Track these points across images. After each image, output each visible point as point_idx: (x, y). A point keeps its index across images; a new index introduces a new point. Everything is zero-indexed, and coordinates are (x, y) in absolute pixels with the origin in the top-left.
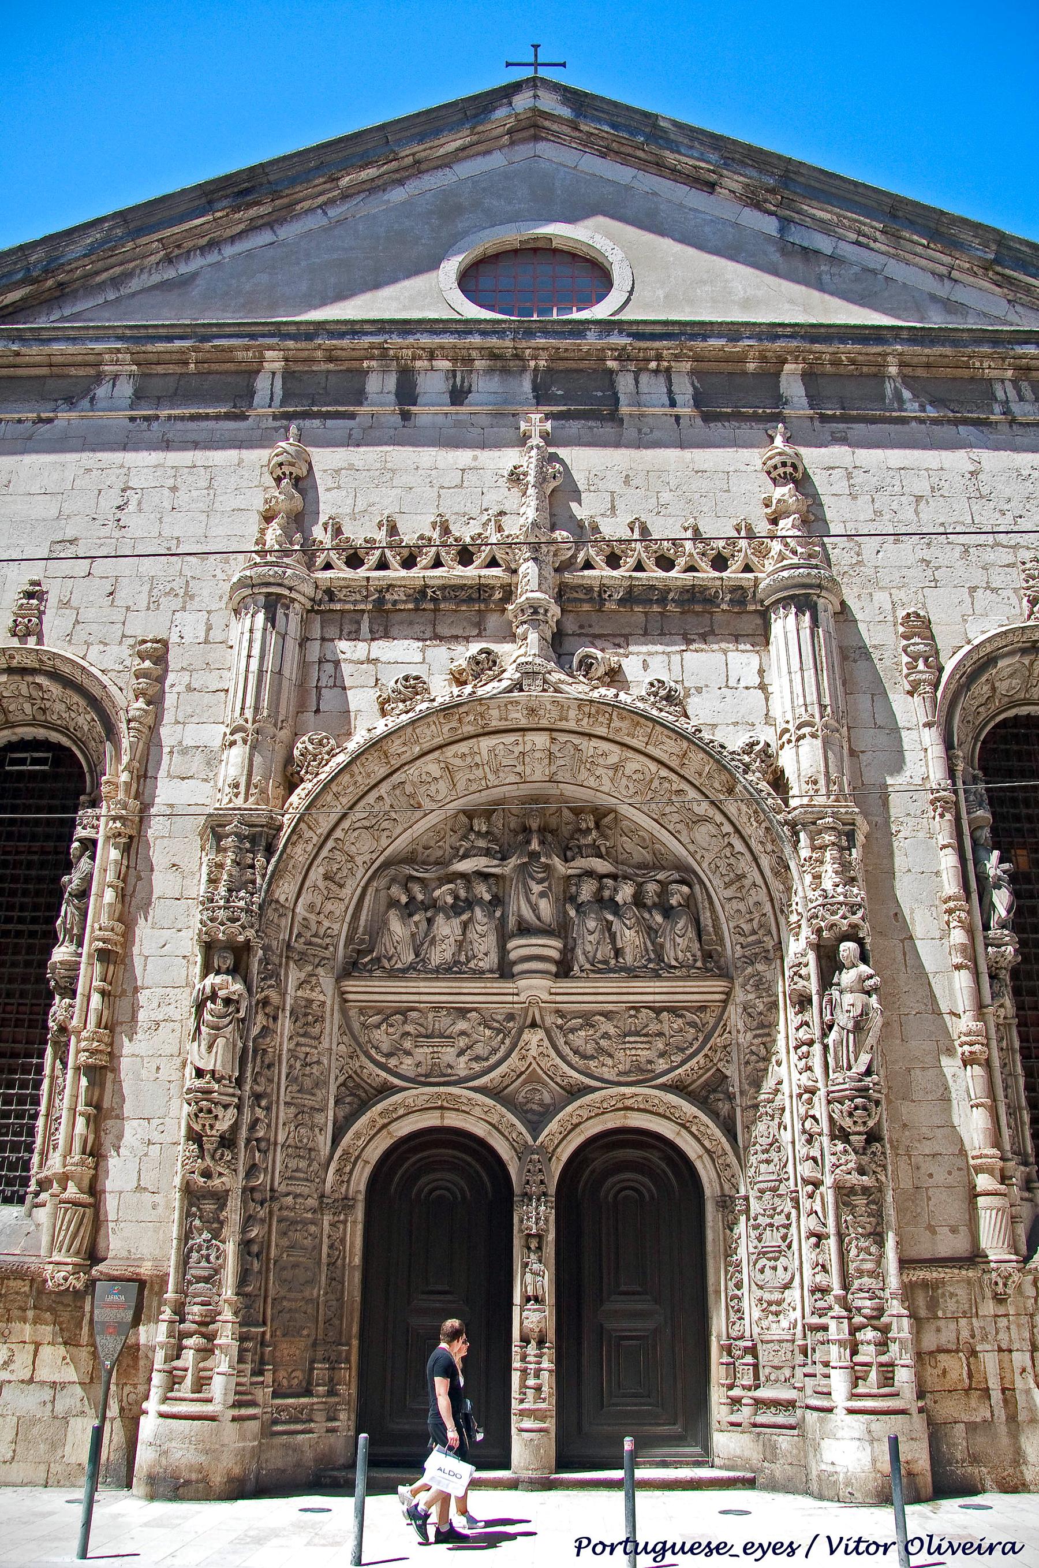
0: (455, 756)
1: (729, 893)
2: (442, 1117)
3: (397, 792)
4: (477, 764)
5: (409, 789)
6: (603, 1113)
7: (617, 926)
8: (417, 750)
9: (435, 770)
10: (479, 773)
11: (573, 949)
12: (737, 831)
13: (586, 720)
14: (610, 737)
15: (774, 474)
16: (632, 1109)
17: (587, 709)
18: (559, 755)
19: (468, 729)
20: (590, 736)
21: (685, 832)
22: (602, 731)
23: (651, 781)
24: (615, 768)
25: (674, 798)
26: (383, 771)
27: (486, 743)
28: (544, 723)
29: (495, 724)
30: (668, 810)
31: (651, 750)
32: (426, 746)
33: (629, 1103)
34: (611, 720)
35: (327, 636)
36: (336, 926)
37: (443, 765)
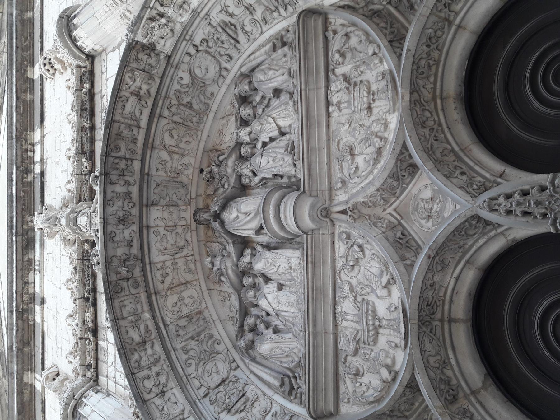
0: (163, 282)
1: (242, 38)
2: (456, 321)
3: (181, 332)
4: (172, 264)
5: (183, 322)
6: (440, 125)
7: (265, 138)
8: (147, 315)
9: (172, 299)
10: (181, 262)
11: (289, 178)
12: (182, 37)
13: (126, 178)
14: (139, 157)
15: (52, 71)
16: (434, 89)
17: (114, 178)
18: (168, 199)
19: (137, 272)
20: (144, 176)
21: (210, 89)
22: (137, 165)
23: (175, 122)
24: (171, 153)
25: (184, 102)
26: (158, 347)
27: (157, 257)
28: (135, 211)
29: (135, 250)
30: (195, 106)
31: (144, 123)
32: (146, 307)
33: (427, 95)
34: (121, 158)
35: (105, 374)
36: (276, 408)
37: (169, 293)
